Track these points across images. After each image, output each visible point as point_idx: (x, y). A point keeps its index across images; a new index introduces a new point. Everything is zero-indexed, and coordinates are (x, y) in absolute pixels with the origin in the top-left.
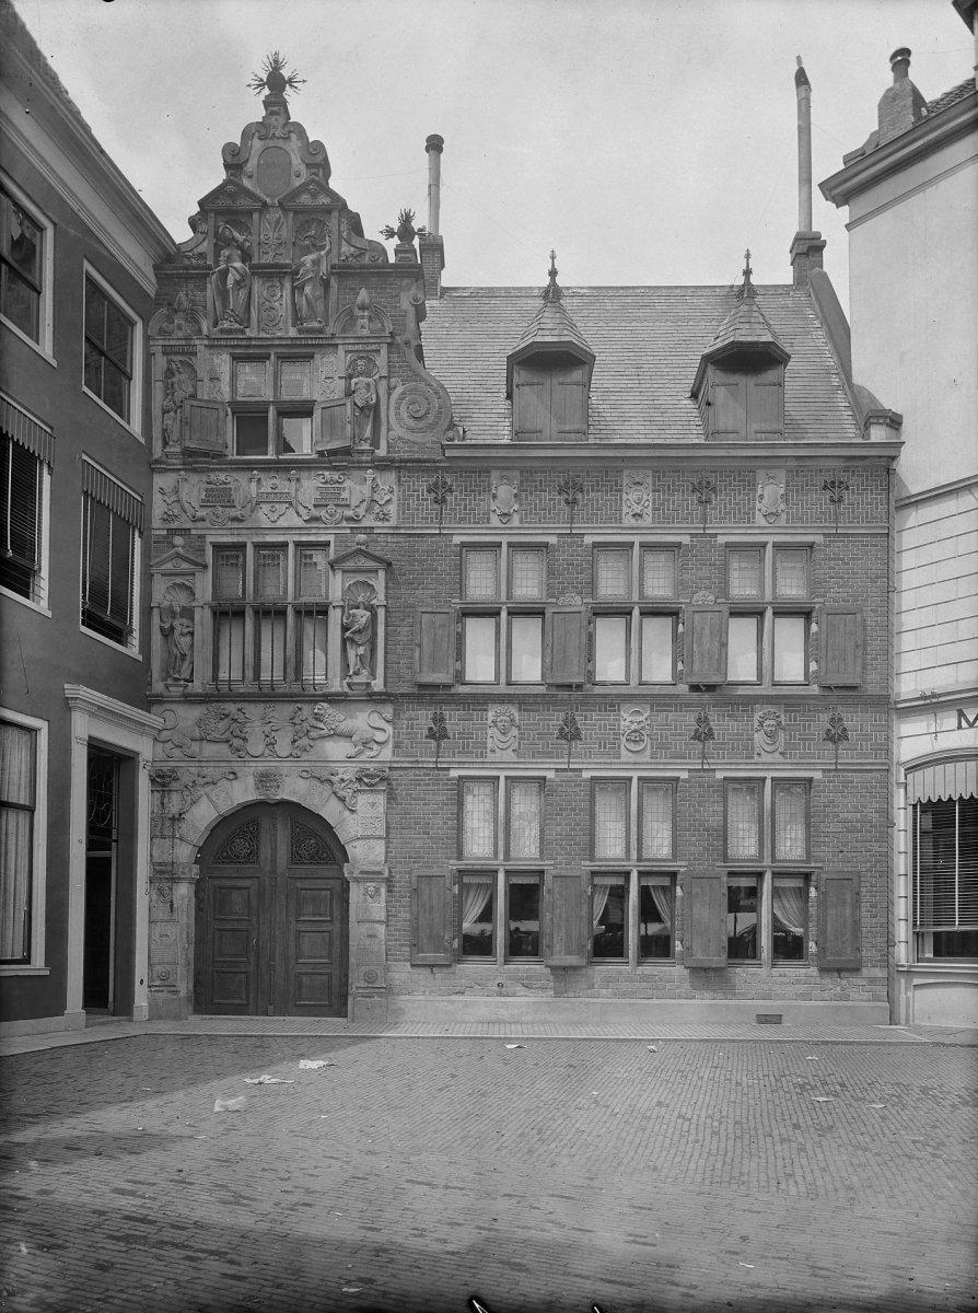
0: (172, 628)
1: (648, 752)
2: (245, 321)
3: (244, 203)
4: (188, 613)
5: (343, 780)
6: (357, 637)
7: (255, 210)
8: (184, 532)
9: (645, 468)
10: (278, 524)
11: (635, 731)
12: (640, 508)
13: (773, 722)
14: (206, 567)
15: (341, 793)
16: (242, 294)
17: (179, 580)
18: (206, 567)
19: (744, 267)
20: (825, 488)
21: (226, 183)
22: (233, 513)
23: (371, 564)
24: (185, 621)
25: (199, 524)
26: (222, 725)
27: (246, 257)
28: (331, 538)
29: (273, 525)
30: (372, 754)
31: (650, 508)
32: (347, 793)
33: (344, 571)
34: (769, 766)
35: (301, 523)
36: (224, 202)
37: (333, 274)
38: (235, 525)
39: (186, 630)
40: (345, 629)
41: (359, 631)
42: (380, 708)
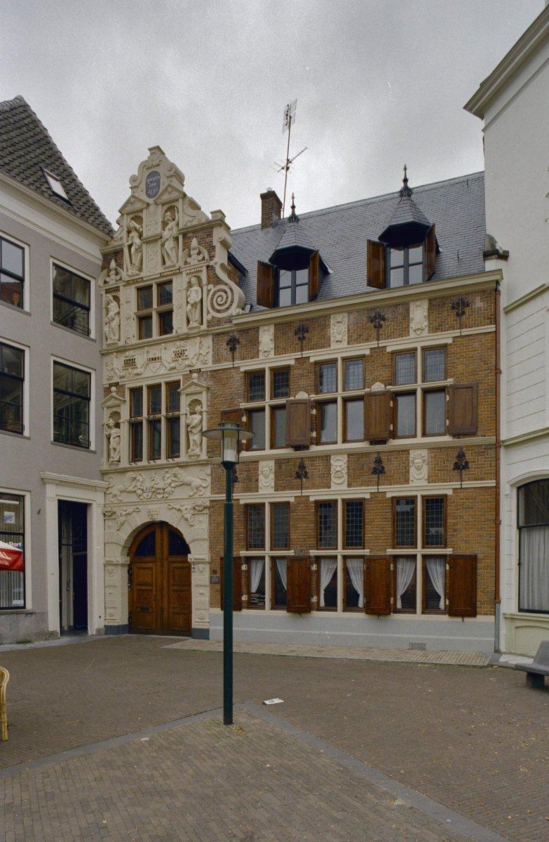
0: (110, 435)
1: (346, 483)
2: (140, 270)
3: (138, 206)
4: (117, 425)
5: (186, 509)
6: (194, 431)
7: (144, 208)
8: (116, 384)
9: (344, 312)
10: (157, 374)
11: (338, 471)
12: (341, 336)
13: (420, 461)
14: (125, 401)
15: (186, 516)
16: (140, 254)
17: (115, 409)
18: (125, 401)
19: (403, 177)
20: (453, 308)
21: (133, 196)
22: (135, 371)
23: (198, 389)
24: (116, 429)
25: (123, 380)
26: (134, 484)
27: (140, 236)
28: (181, 378)
29: (155, 374)
30: (201, 493)
31: (346, 336)
32: (188, 516)
33: (187, 395)
34: (418, 488)
35: (162, 371)
36: (130, 208)
37: (179, 234)
38: (138, 377)
39: (115, 435)
40: (188, 426)
41: (193, 427)
42: (203, 468)
